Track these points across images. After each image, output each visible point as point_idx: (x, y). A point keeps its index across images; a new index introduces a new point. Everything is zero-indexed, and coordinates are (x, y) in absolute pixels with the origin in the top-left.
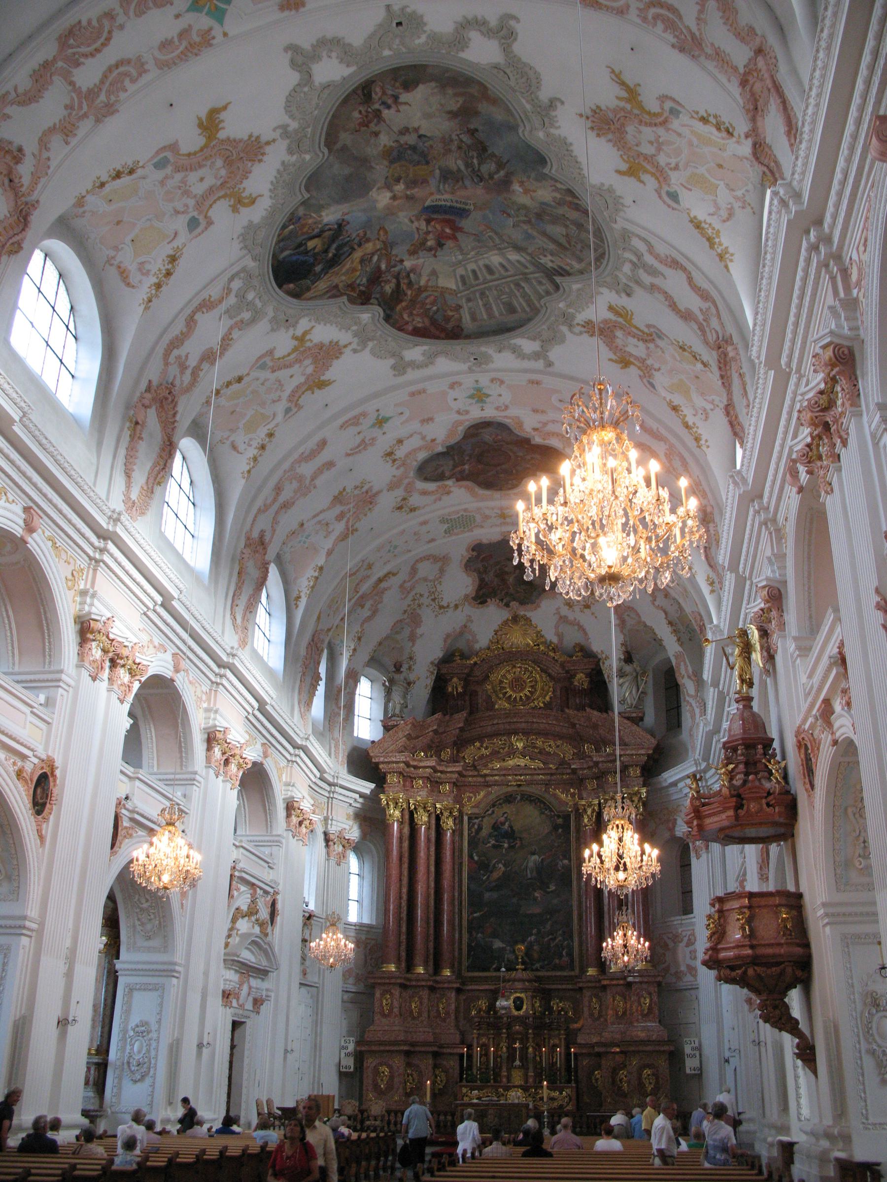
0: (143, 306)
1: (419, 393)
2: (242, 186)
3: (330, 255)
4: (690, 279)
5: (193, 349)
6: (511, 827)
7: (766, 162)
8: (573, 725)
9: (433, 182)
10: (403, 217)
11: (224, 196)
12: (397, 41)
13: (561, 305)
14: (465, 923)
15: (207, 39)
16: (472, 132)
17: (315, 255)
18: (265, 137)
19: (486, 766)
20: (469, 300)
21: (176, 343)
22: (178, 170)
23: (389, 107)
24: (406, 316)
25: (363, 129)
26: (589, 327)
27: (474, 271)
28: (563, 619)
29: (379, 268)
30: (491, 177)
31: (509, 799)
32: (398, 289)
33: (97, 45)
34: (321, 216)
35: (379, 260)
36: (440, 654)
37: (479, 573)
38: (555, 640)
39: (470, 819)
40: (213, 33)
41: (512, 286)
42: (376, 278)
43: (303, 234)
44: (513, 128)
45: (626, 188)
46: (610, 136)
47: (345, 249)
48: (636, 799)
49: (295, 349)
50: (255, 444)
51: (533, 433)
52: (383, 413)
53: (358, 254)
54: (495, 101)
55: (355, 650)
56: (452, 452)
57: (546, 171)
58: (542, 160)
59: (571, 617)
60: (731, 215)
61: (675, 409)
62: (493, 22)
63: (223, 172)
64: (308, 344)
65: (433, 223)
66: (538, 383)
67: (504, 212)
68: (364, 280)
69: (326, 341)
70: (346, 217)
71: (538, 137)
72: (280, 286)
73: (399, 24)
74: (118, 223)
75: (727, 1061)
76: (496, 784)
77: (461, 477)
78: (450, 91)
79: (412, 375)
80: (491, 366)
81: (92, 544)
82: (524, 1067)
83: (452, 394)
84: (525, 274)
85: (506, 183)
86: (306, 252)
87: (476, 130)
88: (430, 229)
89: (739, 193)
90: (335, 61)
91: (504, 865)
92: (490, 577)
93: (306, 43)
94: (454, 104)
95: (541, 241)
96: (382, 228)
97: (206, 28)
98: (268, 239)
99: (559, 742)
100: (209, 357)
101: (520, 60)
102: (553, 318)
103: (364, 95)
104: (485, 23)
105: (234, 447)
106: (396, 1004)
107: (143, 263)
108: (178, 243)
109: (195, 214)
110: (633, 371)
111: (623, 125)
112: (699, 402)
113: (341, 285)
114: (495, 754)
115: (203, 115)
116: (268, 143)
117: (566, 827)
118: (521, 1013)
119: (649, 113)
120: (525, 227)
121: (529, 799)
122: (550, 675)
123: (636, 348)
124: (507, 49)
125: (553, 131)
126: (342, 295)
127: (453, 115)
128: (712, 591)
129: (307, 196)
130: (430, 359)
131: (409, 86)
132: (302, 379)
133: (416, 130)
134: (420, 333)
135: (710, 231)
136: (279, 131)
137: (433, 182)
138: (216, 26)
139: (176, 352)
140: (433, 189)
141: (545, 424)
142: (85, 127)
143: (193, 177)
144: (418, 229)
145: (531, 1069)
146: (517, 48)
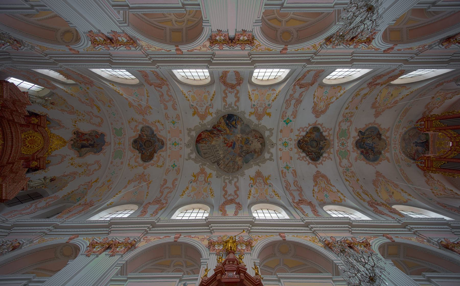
2: (254, 115)
9: (241, 144)
15: (282, 118)
17: (231, 122)
18: (260, 122)
22: (266, 107)
23: (258, 140)
27: (217, 148)
29: (222, 132)
35: (224, 132)
36: (51, 117)
37: (89, 134)
44: (253, 158)
49: (209, 112)
51: (159, 154)
53: (227, 129)
54: (258, 156)
55: (67, 92)
61: (187, 188)
62: (272, 158)
64: (208, 115)
68: (219, 128)
70: (237, 129)
74: (262, 94)
78: (259, 150)
80: (186, 148)
81: (254, 58)
84: (216, 157)
85: (241, 157)
86: (233, 121)
88: (230, 142)
89: (258, 198)
92: (87, 136)
94: (256, 150)
96: (232, 134)
104: (272, 156)
105: (190, 91)
107: (254, 94)
120: (230, 158)
126: (217, 124)
127: (255, 150)
128: (108, 205)
131: (261, 144)
132: (199, 111)
133: (252, 143)
134: (200, 135)
136: (260, 123)
137: (241, 144)
138: (283, 120)
143: (262, 109)
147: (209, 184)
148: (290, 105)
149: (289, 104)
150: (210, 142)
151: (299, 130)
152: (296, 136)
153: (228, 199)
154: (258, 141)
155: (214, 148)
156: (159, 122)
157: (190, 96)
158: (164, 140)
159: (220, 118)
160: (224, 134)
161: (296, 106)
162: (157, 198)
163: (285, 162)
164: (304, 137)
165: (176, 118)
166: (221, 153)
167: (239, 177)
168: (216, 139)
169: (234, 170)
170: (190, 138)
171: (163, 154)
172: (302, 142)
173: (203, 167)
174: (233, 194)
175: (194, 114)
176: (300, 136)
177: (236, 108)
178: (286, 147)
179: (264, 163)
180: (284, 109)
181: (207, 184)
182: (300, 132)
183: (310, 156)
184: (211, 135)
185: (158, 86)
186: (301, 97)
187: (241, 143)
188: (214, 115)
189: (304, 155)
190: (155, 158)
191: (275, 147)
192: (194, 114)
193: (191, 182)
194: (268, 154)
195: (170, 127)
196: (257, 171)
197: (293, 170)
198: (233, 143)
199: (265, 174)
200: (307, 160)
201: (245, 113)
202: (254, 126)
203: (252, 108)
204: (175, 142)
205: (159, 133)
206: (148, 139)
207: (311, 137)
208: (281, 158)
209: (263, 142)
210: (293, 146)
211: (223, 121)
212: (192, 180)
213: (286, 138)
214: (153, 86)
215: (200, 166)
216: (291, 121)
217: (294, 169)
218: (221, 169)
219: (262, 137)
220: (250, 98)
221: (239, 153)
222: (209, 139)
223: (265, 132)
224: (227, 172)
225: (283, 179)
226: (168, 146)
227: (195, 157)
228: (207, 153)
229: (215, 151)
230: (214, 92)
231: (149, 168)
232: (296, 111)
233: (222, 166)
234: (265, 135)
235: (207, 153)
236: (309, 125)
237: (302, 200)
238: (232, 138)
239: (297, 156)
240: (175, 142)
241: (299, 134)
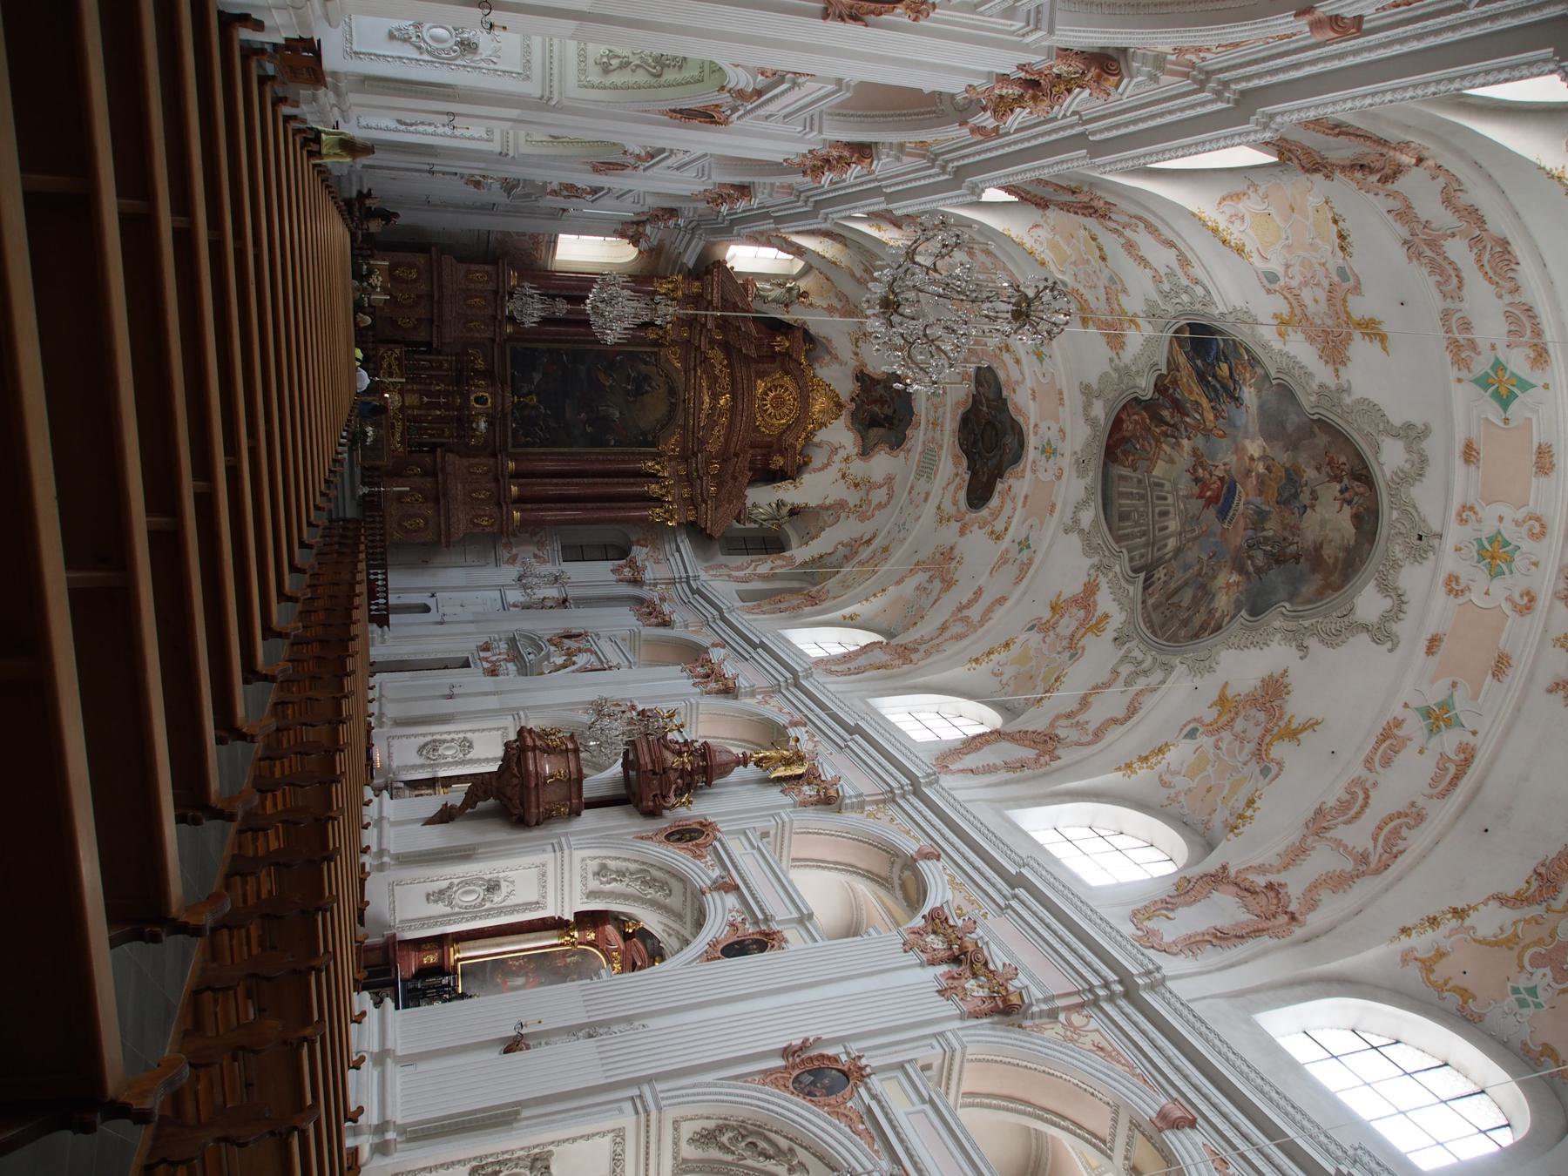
0: (1196, 211)
1: (1061, 399)
4: (1115, 721)
5: (1142, 238)
6: (647, 392)
7: (1197, 887)
8: (737, 455)
10: (1231, 458)
13: (1117, 568)
14: (556, 346)
16: (1297, 558)
19: (704, 372)
20: (1140, 481)
21: (1149, 226)
23: (1341, 492)
24: (1136, 417)
26: (1091, 589)
28: (835, 451)
29: (1188, 415)
30: (1250, 557)
31: (672, 391)
32: (1161, 421)
33: (1491, 274)
38: (816, 439)
39: (654, 353)
40: (1466, 371)
42: (1178, 407)
44: (1291, 598)
45: (1210, 686)
48: (667, 516)
49: (1124, 313)
50: (1037, 246)
51: (1006, 486)
52: (1047, 360)
53: (1204, 402)
54: (1320, 594)
56: (1000, 403)
57: (1243, 613)
58: (1255, 612)
59: (836, 458)
60: (1165, 784)
61: (1007, 645)
62: (1395, 627)
66: (1052, 512)
70: (1244, 408)
71: (1275, 620)
73: (1420, 538)
75: (433, 596)
76: (688, 380)
77: (976, 399)
78: (1341, 555)
79: (1079, 399)
80: (1074, 474)
82: (421, 406)
83: (1055, 428)
85: (1241, 570)
86: (1217, 359)
87: (1298, 563)
89: (1182, 798)
91: (611, 386)
93: (1425, 445)
94: (1327, 553)
95: (1180, 578)
96: (1225, 435)
98: (1242, 334)
99: (722, 439)
100: (1130, 246)
106: (480, 286)
107: (1243, 218)
108: (1256, 259)
109: (1282, 282)
110: (1046, 614)
111: (1266, 710)
112: (1009, 672)
114: (714, 380)
115: (1384, 328)
116: (1337, 370)
117: (646, 444)
118: (473, 403)
119: (1270, 744)
120: (1196, 568)
121: (672, 409)
122: (785, 432)
123: (1067, 625)
124: (1365, 628)
127: (1318, 548)
128: (845, 617)
129: (1274, 382)
130: (1091, 422)
131: (1357, 519)
133: (1313, 507)
134: (1117, 424)
135: (1154, 760)
136: (1346, 385)
137: (1258, 500)
138: (1470, 376)
139: (1141, 225)
140: (1251, 498)
141: (1013, 500)
142: (1404, 232)
145: (420, 412)
160: (1193, 427)
163: (1446, 681)
166: (1173, 525)
167: (1180, 669)
169: (1182, 633)
178: (1495, 573)
179: (1331, 645)
188: (1148, 330)
190: (994, 502)
194: (1379, 596)
199: (1298, 707)
202: (1319, 394)
208: (1433, 644)
209: (1367, 509)
216: (1525, 386)
219: (1362, 475)
221: (1241, 546)
224: (1154, 633)
238: (1225, 460)
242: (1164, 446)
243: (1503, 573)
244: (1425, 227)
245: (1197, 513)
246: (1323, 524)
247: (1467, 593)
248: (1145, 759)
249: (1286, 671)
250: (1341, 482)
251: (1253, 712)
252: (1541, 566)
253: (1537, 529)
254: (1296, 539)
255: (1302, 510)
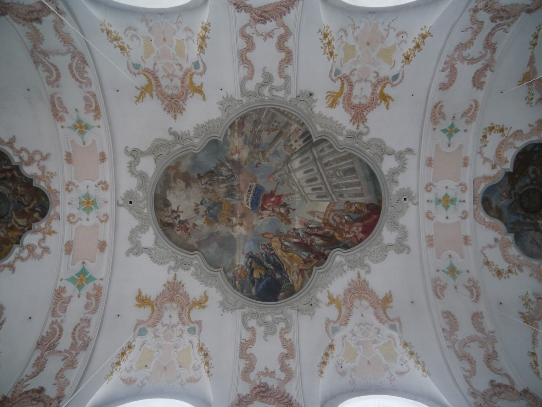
3: (271, 267)
10: (257, 221)
11: (190, 309)
12: (140, 205)
15: (98, 289)
16: (200, 177)
17: (266, 275)
18: (170, 277)
22: (154, 325)
23: (179, 216)
24: (348, 236)
25: (189, 231)
27: (313, 189)
29: (295, 243)
34: (239, 265)
35: (289, 242)
40: (97, 284)
41: (327, 168)
42: (304, 246)
43: (246, 276)
44: (195, 156)
46: (181, 103)
47: (271, 258)
49: (339, 308)
50: (406, 357)
51: (499, 168)
53: (279, 252)
54: (178, 164)
57: (221, 140)
61: (407, 58)
62: (131, 159)
63: (175, 305)
65: (266, 207)
67: (257, 166)
68: (307, 254)
69: (347, 287)
70: (246, 252)
71: (198, 142)
72: (277, 300)
73: (131, 202)
78: (173, 185)
80: (414, 189)
84: (315, 159)
85: (233, 162)
86: (260, 280)
87: (198, 175)
88: (271, 209)
89: (175, 27)
90: (143, 236)
93: (129, 246)
94: (182, 184)
96: (263, 235)
97: (93, 286)
98: (235, 296)
101: (150, 148)
102: (357, 145)
103: (167, 226)
104: (130, 163)
105: (401, 373)
109: (187, 327)
111: (168, 96)
112: (392, 40)
113: (301, 267)
116: (175, 279)
120: (267, 155)
124: (144, 154)
125: (192, 134)
126: (312, 269)
127: (188, 185)
131: (167, 204)
132: (372, 310)
133: (197, 205)
134: (368, 230)
137: (234, 202)
138: (96, 282)
140: (239, 202)
143: (165, 319)
144: (269, 216)
146: (143, 149)
147: (338, 72)
148: (73, 334)
149: (76, 336)
150: (337, 207)
151: (46, 250)
152: (54, 232)
153: (274, 22)
154: (176, 212)
155: (320, 189)
156: (499, 273)
157: (401, 359)
158: (482, 214)
159: (302, 287)
161: (54, 329)
162: (506, 27)
164: (30, 229)
165: (443, 288)
166: (300, 176)
167: (238, 96)
168: (316, 219)
169: (255, 117)
170: (402, 221)
171: (486, 170)
172: (33, 210)
173: (358, 126)
174: (258, 41)
175: (388, 299)
176: (40, 230)
177: (252, 323)
180: (95, 319)
181: (345, 71)
182: (43, 245)
183: (8, 167)
184: (331, 232)
185: (503, 389)
186: (38, 359)
187: (233, 206)
189: (29, 170)
190: (510, 154)
191: (122, 193)
192: (388, 299)
193: (395, 77)
195: (462, 257)
196: (179, 116)
197: (61, 119)
198: (260, 205)
200: (18, 152)
201: (222, 304)
202: (191, 264)
203: (199, 323)
204: (447, 207)
205: (499, 237)
206: (532, 216)
207: (7, 228)
209: (162, 210)
210: (64, 198)
211: (294, 278)
212: (393, 86)
213: (85, 223)
214: (520, 388)
215: (365, 130)
216: (72, 280)
217: (59, 124)
218: (298, 122)
220: (206, 355)
222: (338, 220)
223: (156, 243)
224: (279, 110)
225: (95, 88)
226: (468, 196)
227: (382, 160)
228: (346, 172)
229: (319, 181)
230: (322, 372)
231: (530, 126)
232: (54, 314)
233: (296, 131)
234: (155, 234)
235: (346, 172)
236: (11, 267)
237: (31, 20)
239: (51, 166)
240: (447, 207)
241: (44, 239)
242: (321, 221)
243: (83, 197)
244: (67, 357)
245: (279, 186)
246: (188, 198)
247: (97, 184)
248: (203, 38)
249: (175, 119)
250: (180, 222)
251: (175, 92)
252: (67, 204)
253: (71, 218)
254: (204, 186)
255: (204, 202)
